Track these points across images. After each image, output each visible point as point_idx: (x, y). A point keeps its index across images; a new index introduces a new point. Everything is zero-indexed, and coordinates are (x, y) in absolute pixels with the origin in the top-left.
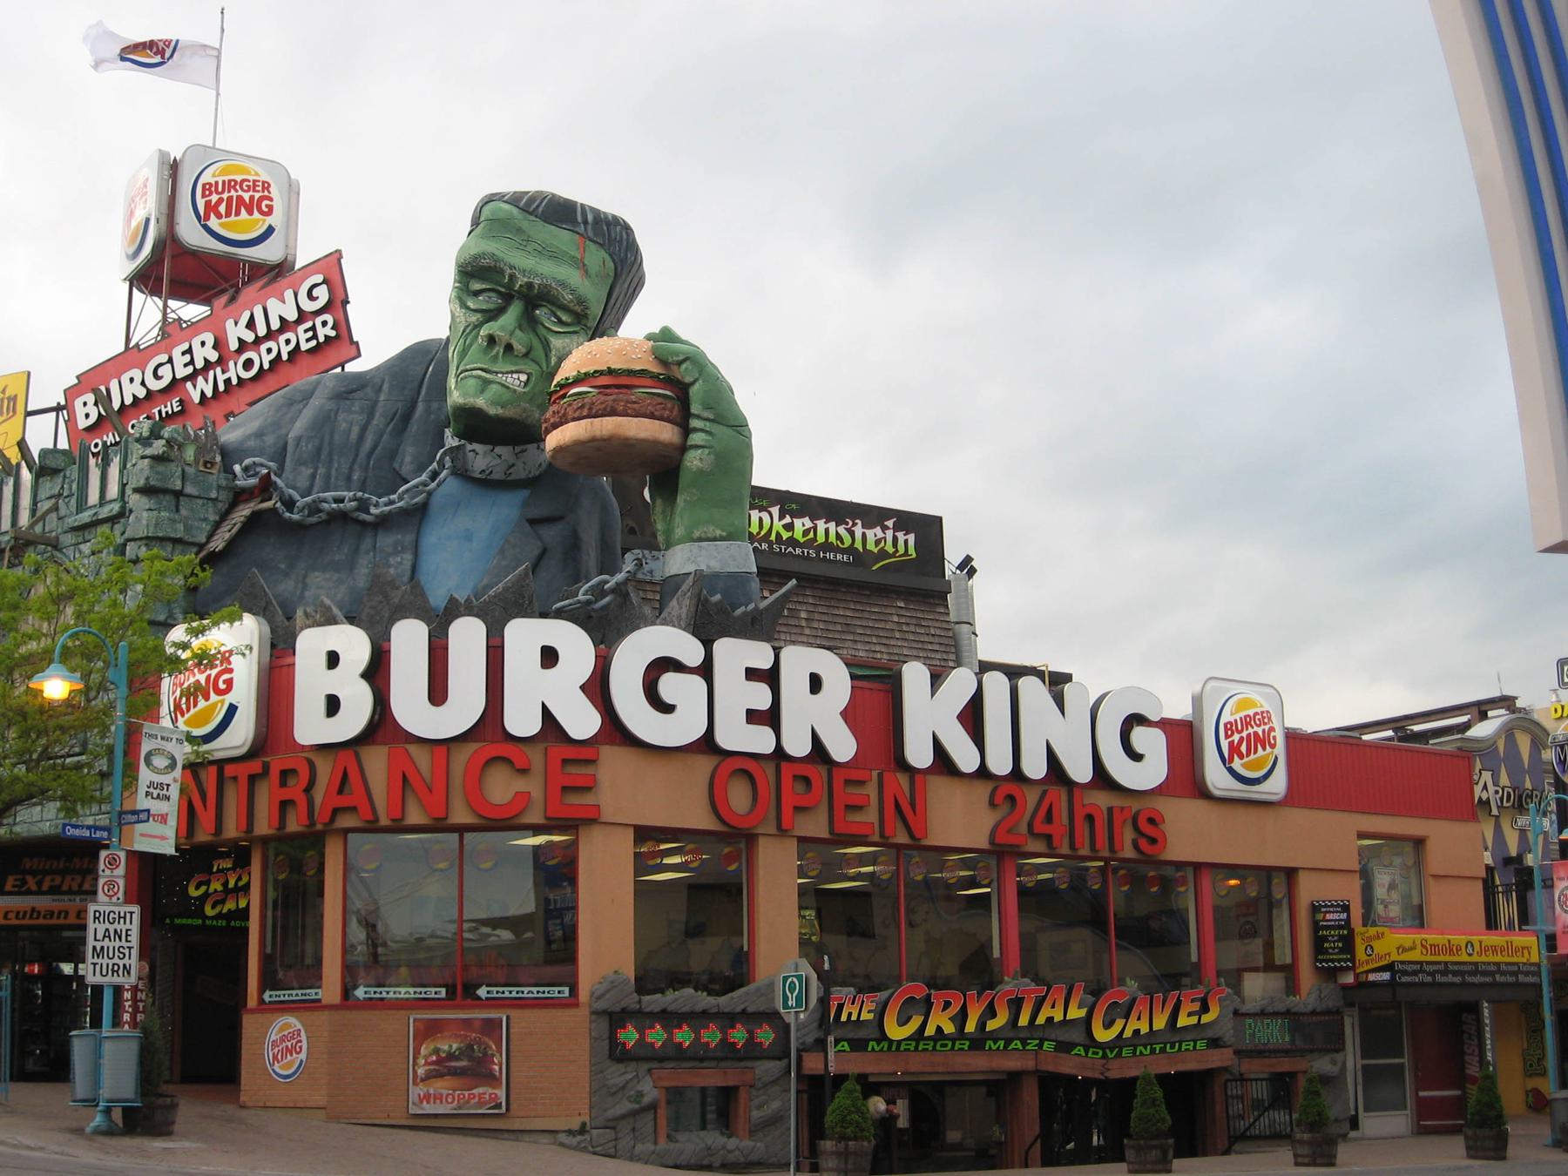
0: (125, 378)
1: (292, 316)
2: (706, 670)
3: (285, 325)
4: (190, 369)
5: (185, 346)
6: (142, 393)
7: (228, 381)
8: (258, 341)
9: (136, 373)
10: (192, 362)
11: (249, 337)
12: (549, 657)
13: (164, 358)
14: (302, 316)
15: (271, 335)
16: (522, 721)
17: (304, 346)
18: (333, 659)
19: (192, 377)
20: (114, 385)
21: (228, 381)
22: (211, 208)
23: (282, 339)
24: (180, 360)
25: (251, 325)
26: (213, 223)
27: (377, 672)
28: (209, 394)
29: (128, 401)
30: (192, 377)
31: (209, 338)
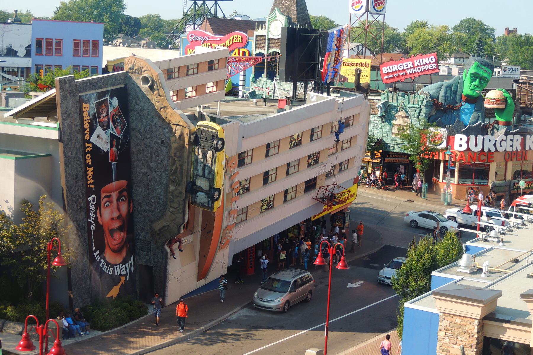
0: (393, 66)
1: (428, 63)
2: (506, 141)
3: (426, 64)
4: (407, 68)
5: (406, 63)
6: (397, 70)
7: (415, 71)
8: (421, 66)
9: (396, 66)
10: (407, 66)
11: (419, 64)
12: (490, 141)
13: (402, 64)
14: (430, 63)
15: (423, 65)
16: (486, 150)
17: (430, 69)
18: (461, 139)
19: (408, 69)
20: (391, 67)
21: (415, 71)
22: (376, 5)
23: (426, 66)
24: (405, 66)
25: (420, 62)
26: (376, 8)
27: (468, 142)
28: (411, 73)
29: (394, 70)
30: (408, 69)
31: (411, 63)
